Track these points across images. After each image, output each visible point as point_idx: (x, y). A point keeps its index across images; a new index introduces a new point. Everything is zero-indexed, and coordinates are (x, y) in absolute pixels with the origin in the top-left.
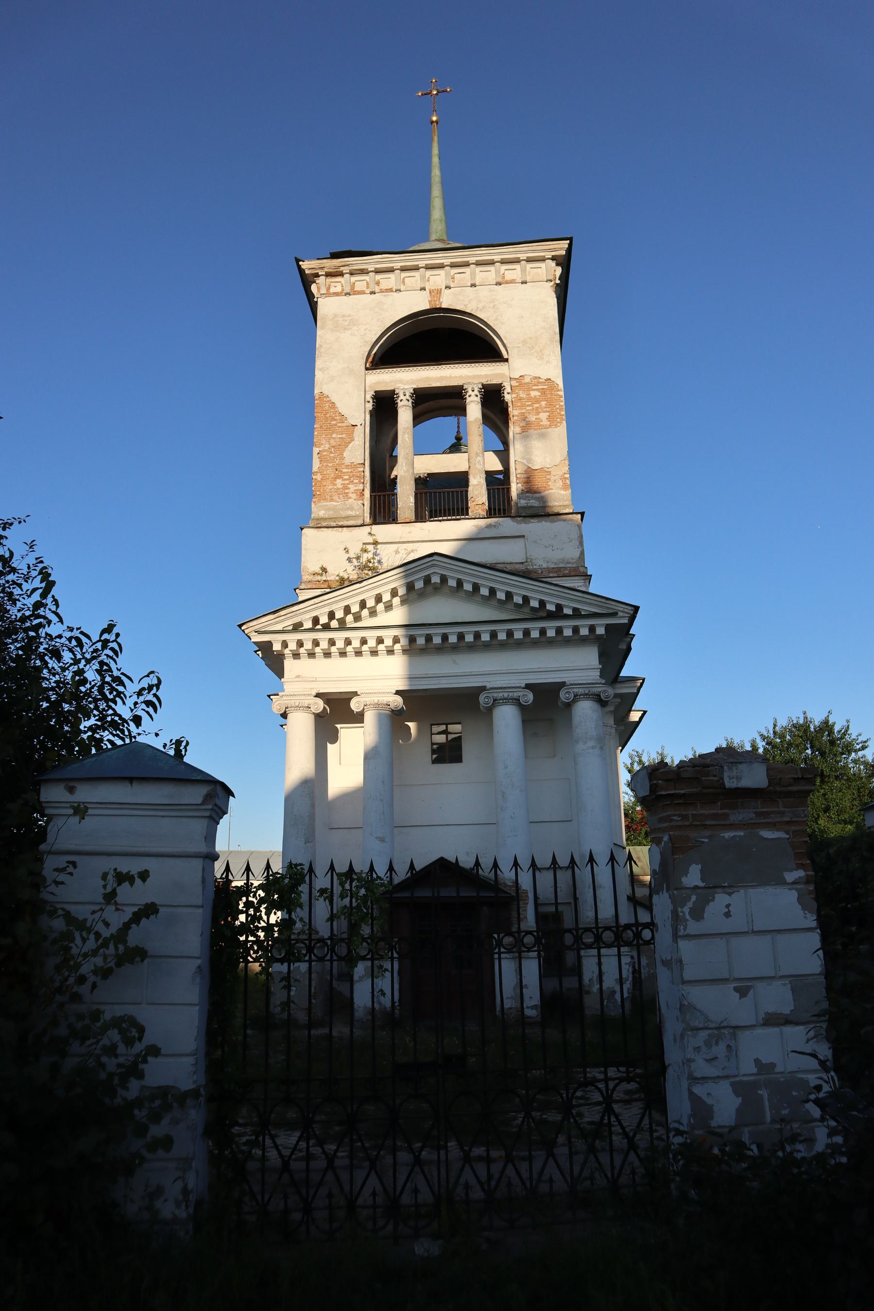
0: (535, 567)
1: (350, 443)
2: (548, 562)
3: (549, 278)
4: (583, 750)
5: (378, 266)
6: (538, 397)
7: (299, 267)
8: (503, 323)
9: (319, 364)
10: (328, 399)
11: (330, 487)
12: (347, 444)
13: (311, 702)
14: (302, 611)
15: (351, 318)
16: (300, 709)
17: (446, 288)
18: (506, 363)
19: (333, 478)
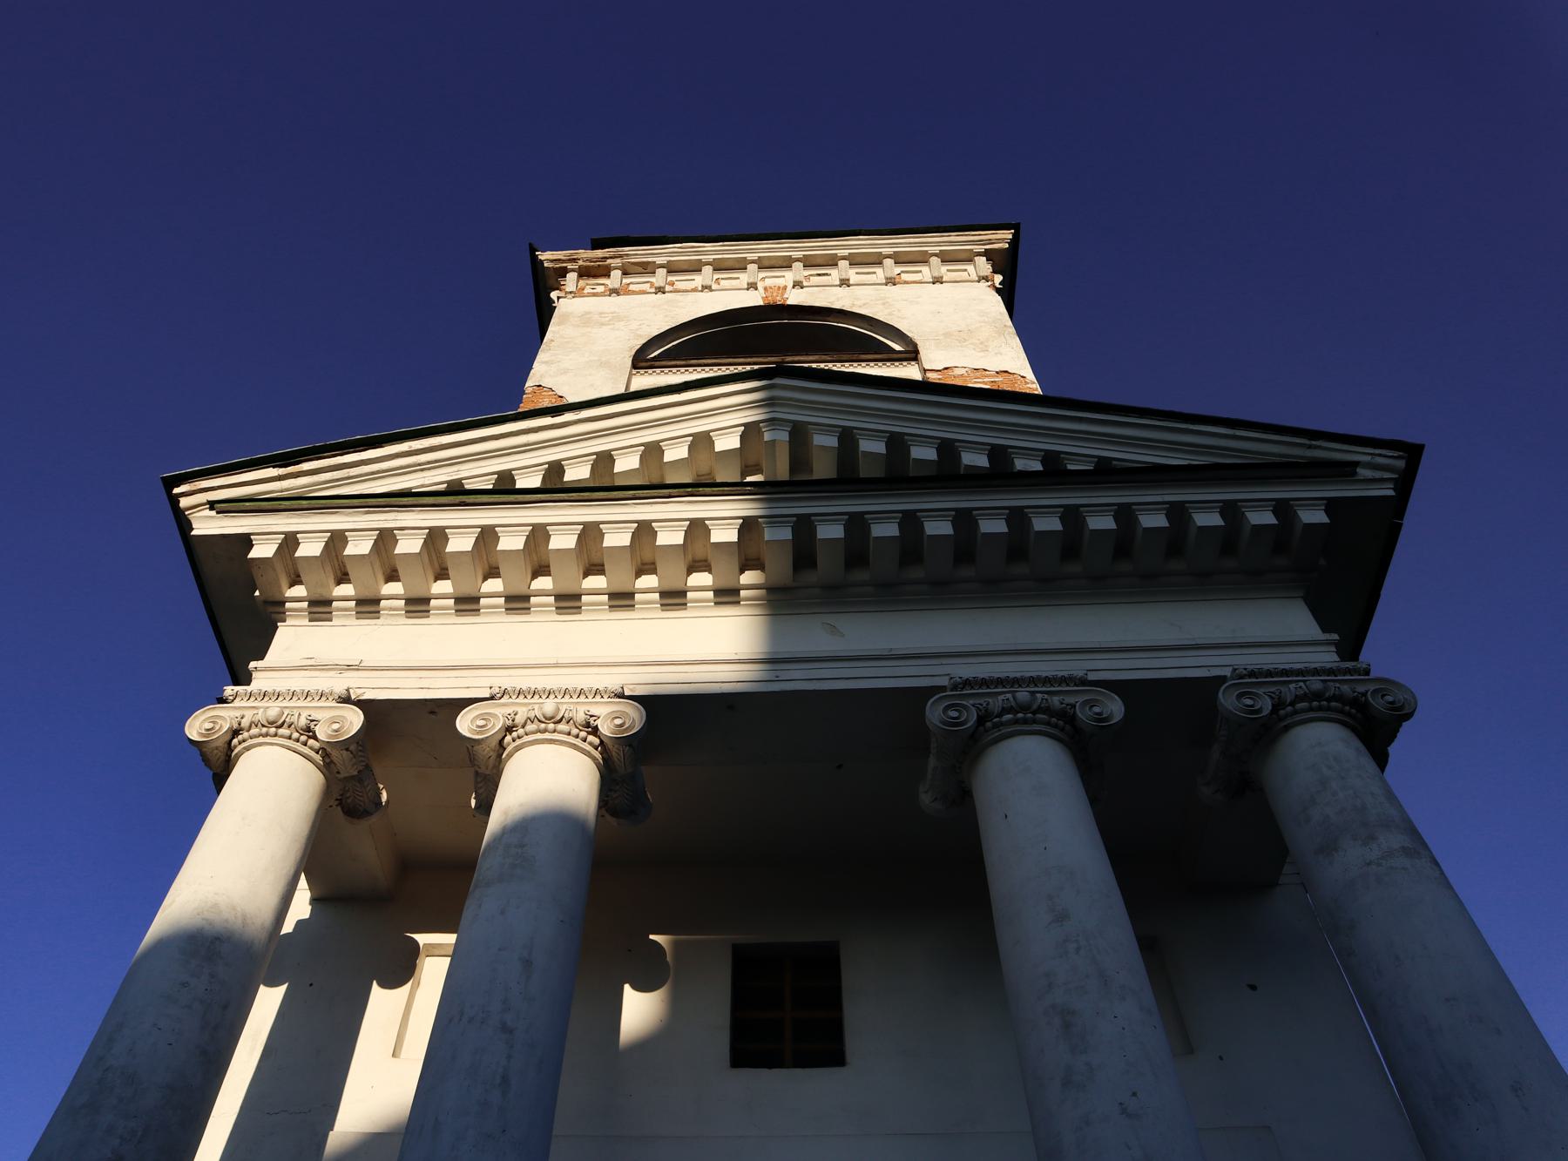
3: (982, 274)
4: (1369, 864)
7: (534, 259)
16: (281, 731)
17: (793, 287)
18: (913, 363)
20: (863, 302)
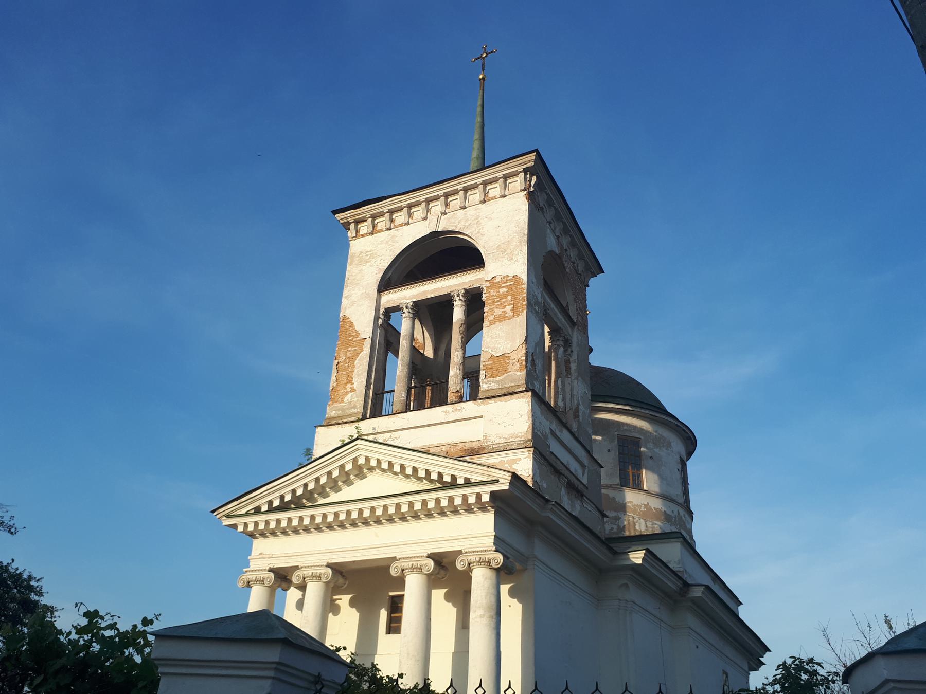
0: (489, 443)
1: (360, 353)
2: (500, 438)
5: (390, 208)
6: (506, 293)
8: (483, 235)
9: (346, 292)
10: (349, 320)
11: (342, 391)
12: (358, 354)
13: (266, 576)
14: (255, 498)
15: (372, 252)
19: (345, 384)
20: (469, 222)
